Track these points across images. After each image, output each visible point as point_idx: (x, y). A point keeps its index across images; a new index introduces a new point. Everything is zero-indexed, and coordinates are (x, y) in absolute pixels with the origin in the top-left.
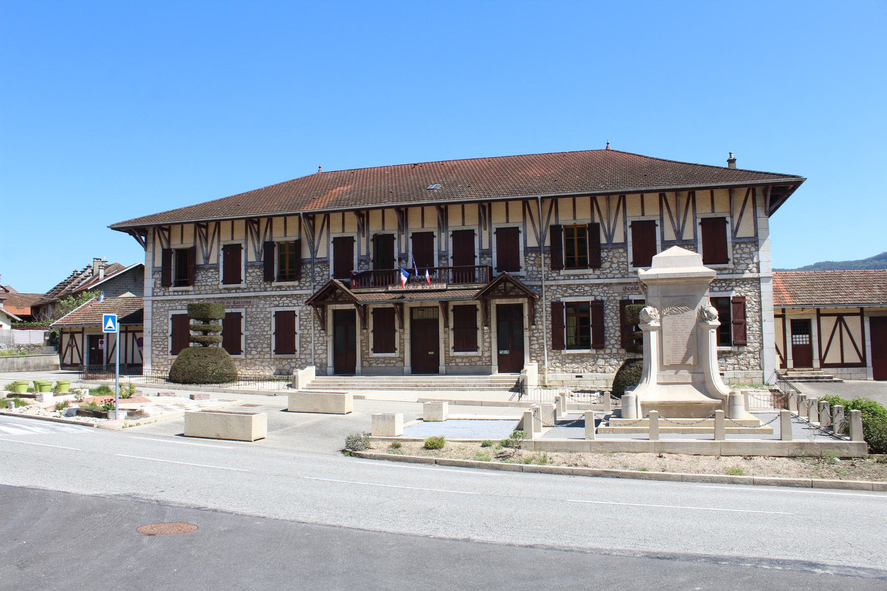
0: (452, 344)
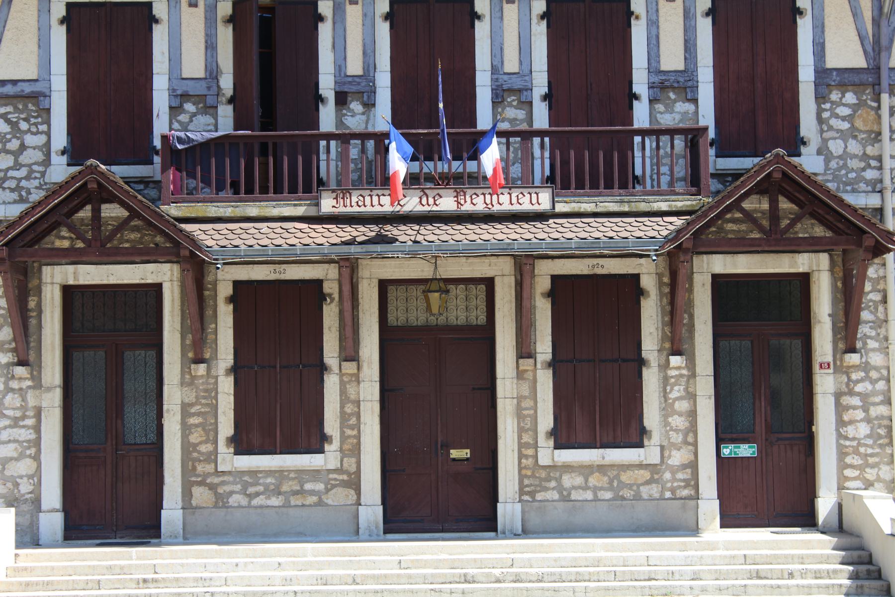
0: (546, 420)
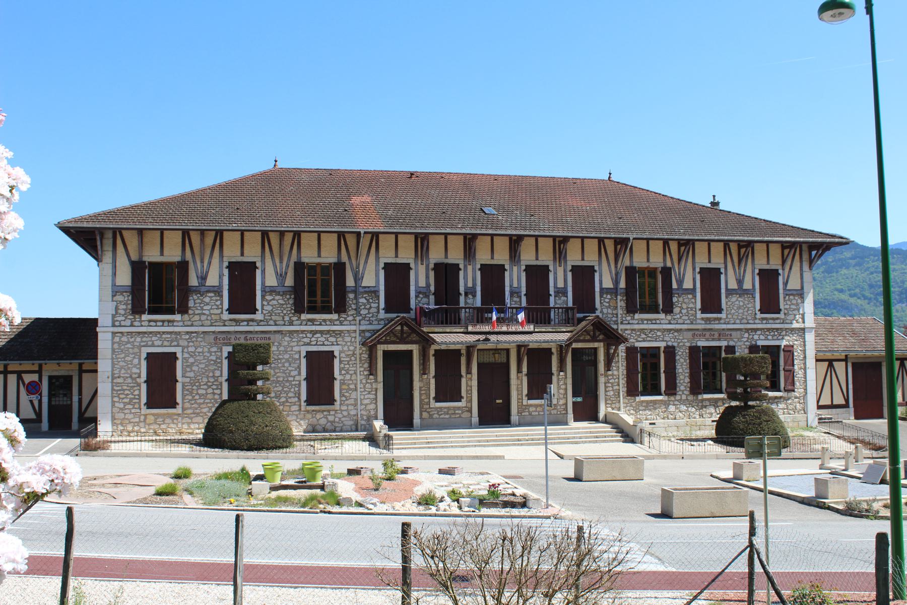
0: (525, 392)
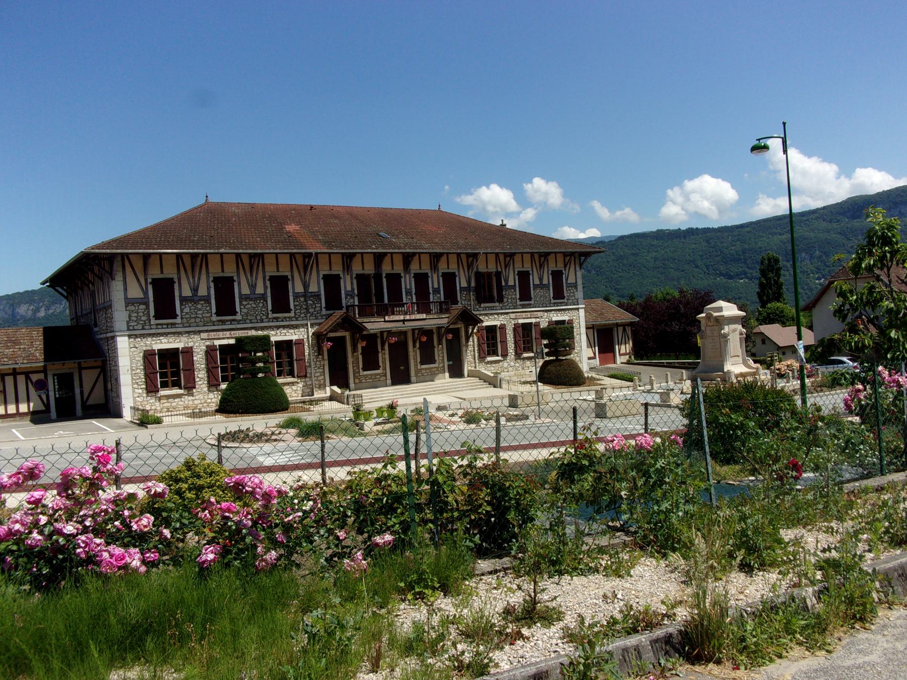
0: (419, 360)
